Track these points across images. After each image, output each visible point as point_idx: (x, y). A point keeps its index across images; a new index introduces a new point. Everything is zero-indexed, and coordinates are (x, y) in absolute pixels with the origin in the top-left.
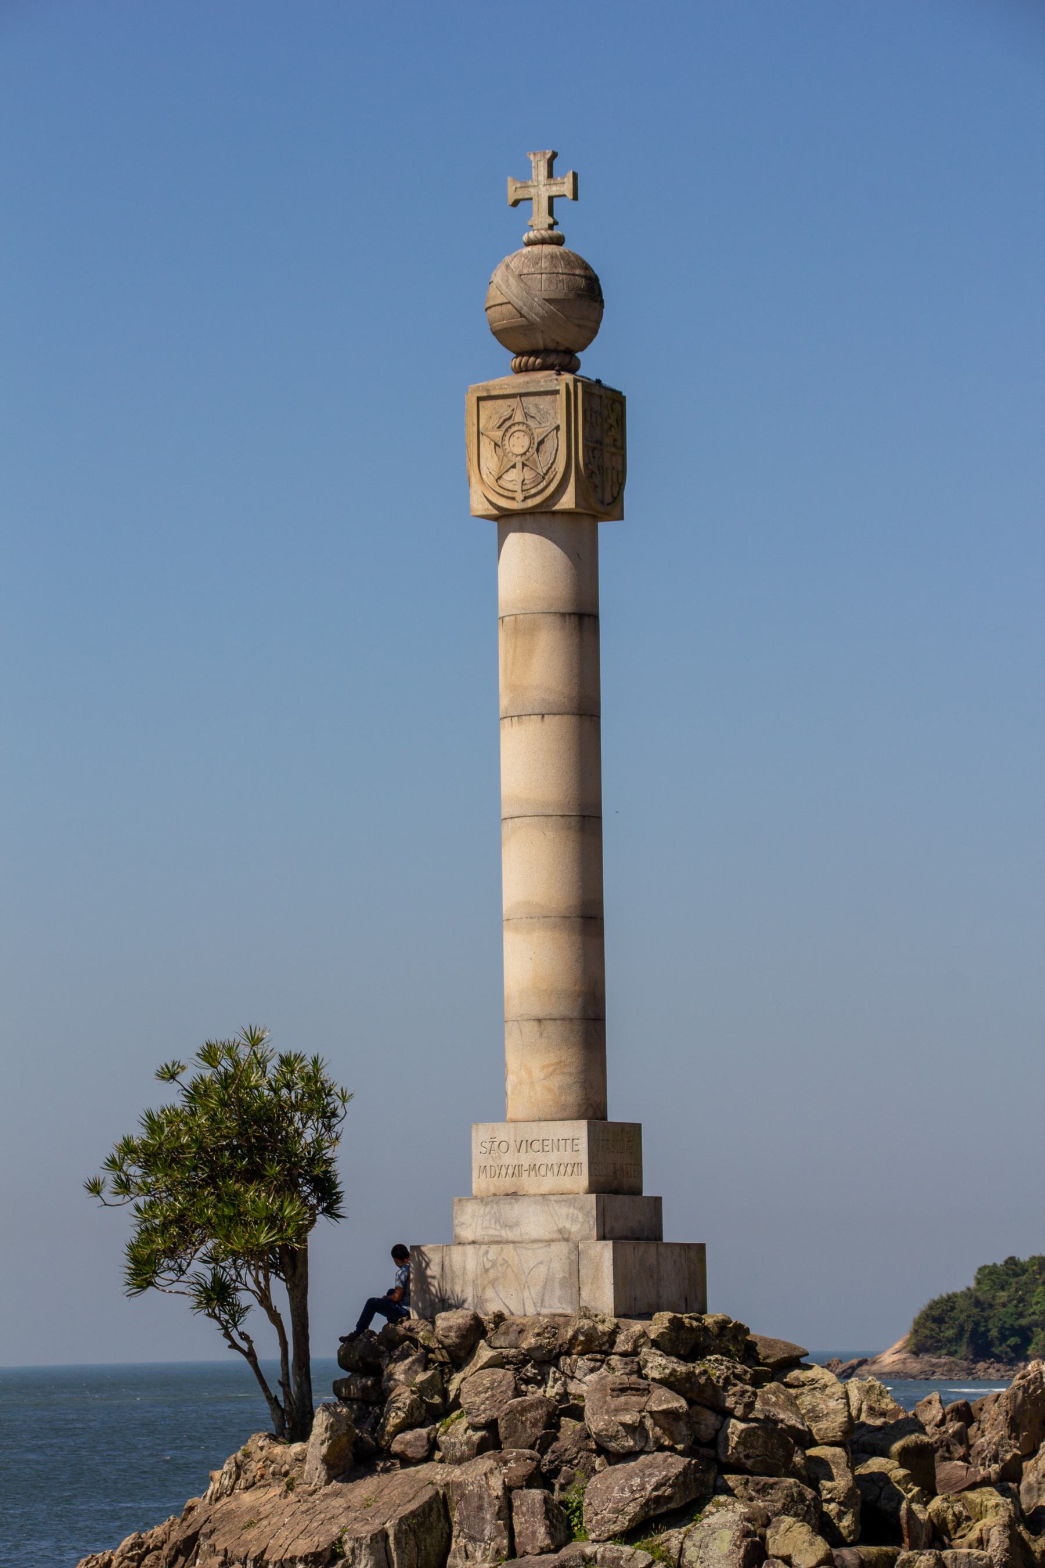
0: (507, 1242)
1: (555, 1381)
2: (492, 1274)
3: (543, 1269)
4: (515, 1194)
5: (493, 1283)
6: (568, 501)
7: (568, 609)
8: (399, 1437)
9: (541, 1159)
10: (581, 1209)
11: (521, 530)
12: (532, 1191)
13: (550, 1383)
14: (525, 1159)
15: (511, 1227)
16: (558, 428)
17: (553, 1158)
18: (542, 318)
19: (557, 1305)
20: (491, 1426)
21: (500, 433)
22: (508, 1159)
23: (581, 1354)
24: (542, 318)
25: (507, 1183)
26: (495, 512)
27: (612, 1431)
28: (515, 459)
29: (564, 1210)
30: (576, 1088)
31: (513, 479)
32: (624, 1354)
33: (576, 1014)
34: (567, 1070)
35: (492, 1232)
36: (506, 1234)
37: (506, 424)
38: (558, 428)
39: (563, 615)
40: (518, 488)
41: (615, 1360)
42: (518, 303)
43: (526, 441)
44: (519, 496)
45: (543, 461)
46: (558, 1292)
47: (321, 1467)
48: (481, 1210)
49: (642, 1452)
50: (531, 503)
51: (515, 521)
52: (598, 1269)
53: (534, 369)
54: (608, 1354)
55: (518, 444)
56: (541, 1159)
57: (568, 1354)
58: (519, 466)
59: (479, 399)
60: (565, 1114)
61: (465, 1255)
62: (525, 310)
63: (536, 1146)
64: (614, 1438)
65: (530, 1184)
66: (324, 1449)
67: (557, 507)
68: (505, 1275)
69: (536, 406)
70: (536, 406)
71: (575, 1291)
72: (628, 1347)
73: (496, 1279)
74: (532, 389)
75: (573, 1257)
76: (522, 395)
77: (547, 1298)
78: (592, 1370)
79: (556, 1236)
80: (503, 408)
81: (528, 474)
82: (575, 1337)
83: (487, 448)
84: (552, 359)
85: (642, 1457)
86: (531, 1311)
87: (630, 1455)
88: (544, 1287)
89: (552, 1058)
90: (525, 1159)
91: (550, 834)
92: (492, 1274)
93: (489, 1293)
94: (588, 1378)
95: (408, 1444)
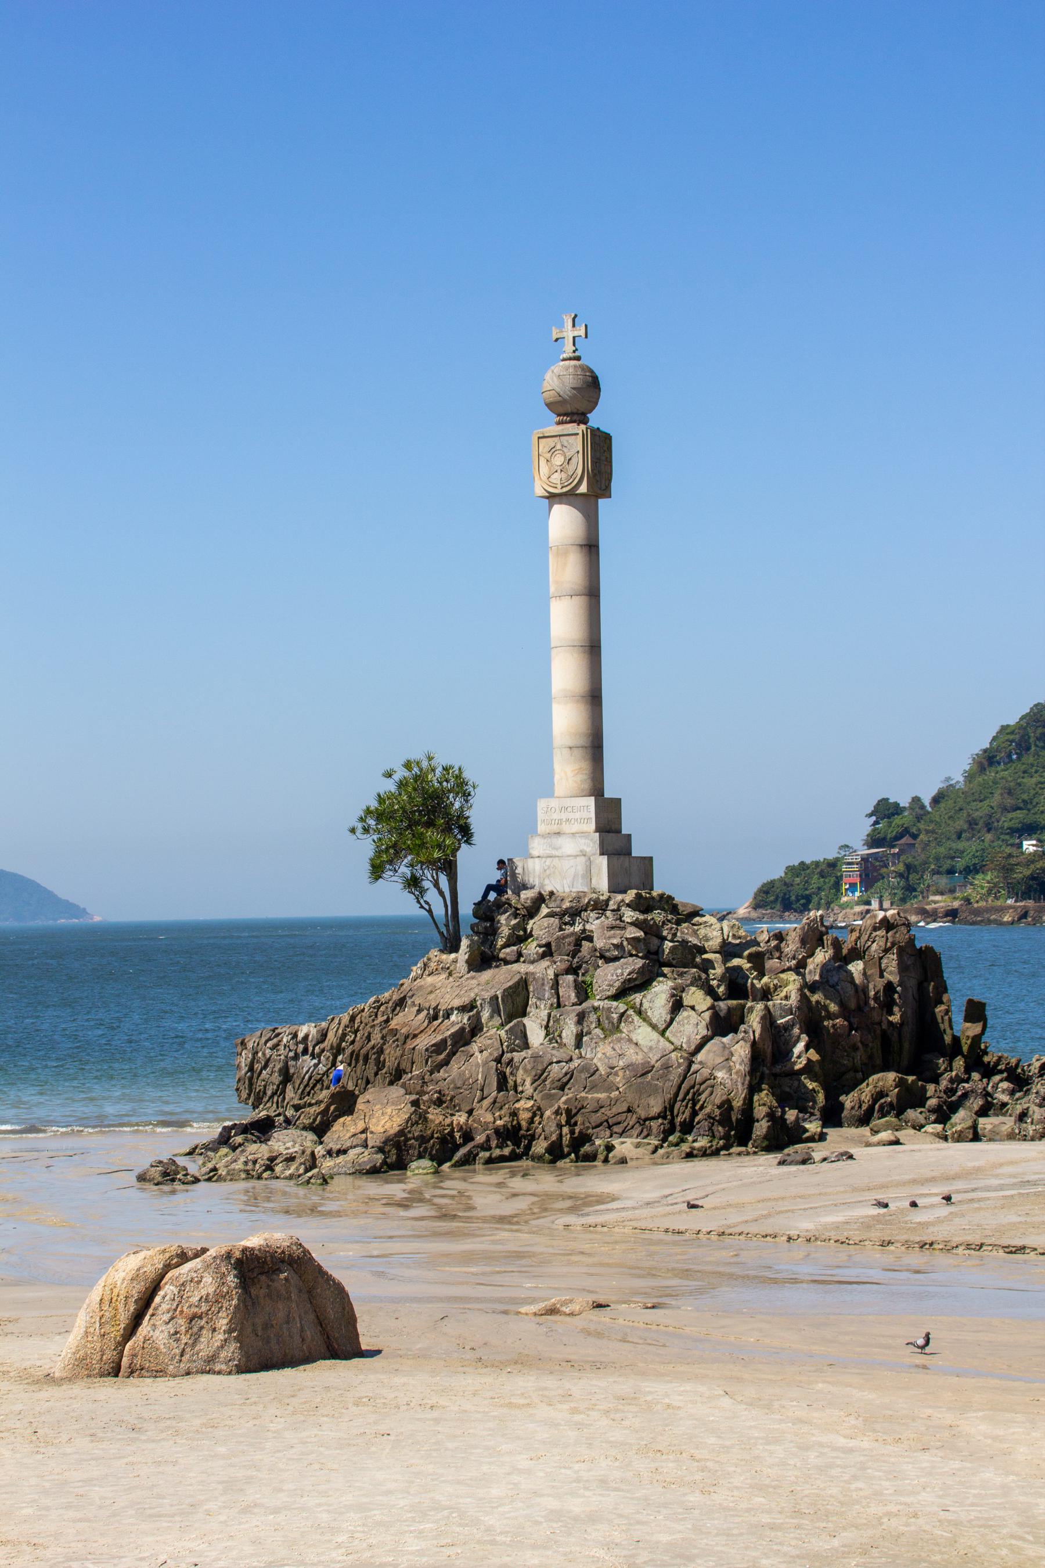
0: (555, 857)
1: (579, 923)
2: (548, 872)
3: (573, 870)
4: (559, 833)
5: (549, 876)
6: (583, 489)
7: (584, 543)
8: (503, 951)
9: (571, 816)
10: (592, 840)
11: (561, 503)
12: (567, 832)
13: (577, 924)
14: (564, 816)
15: (557, 849)
16: (578, 452)
17: (578, 815)
18: (570, 397)
19: (580, 887)
20: (548, 945)
21: (549, 455)
22: (555, 816)
23: (592, 910)
24: (570, 397)
25: (555, 828)
26: (547, 494)
27: (607, 947)
28: (556, 468)
29: (583, 841)
30: (589, 781)
31: (556, 478)
32: (613, 911)
33: (588, 744)
34: (584, 772)
35: (548, 852)
36: (555, 853)
37: (552, 450)
38: (578, 452)
39: (581, 546)
40: (559, 482)
41: (608, 913)
42: (558, 390)
43: (562, 459)
44: (559, 486)
45: (571, 469)
46: (580, 881)
47: (465, 965)
48: (542, 841)
49: (622, 957)
50: (565, 490)
51: (557, 499)
52: (600, 870)
53: (566, 423)
54: (605, 910)
55: (558, 460)
56: (571, 816)
57: (586, 910)
58: (559, 471)
59: (539, 438)
60: (584, 794)
61: (534, 863)
62: (561, 393)
63: (569, 809)
64: (608, 950)
65: (566, 828)
66: (467, 957)
67: (578, 492)
68: (554, 873)
69: (567, 441)
70: (567, 441)
71: (589, 880)
72: (615, 907)
73: (550, 875)
74: (565, 433)
75: (588, 864)
76: (560, 436)
77: (575, 883)
78: (597, 918)
79: (579, 853)
80: (551, 442)
81: (564, 475)
82: (589, 902)
83: (543, 462)
84: (575, 417)
85: (622, 960)
86: (567, 890)
87: (616, 959)
88: (573, 879)
89: (577, 766)
90: (564, 816)
91: (576, 655)
92: (548, 872)
93: (547, 882)
94: (596, 922)
95: (507, 954)
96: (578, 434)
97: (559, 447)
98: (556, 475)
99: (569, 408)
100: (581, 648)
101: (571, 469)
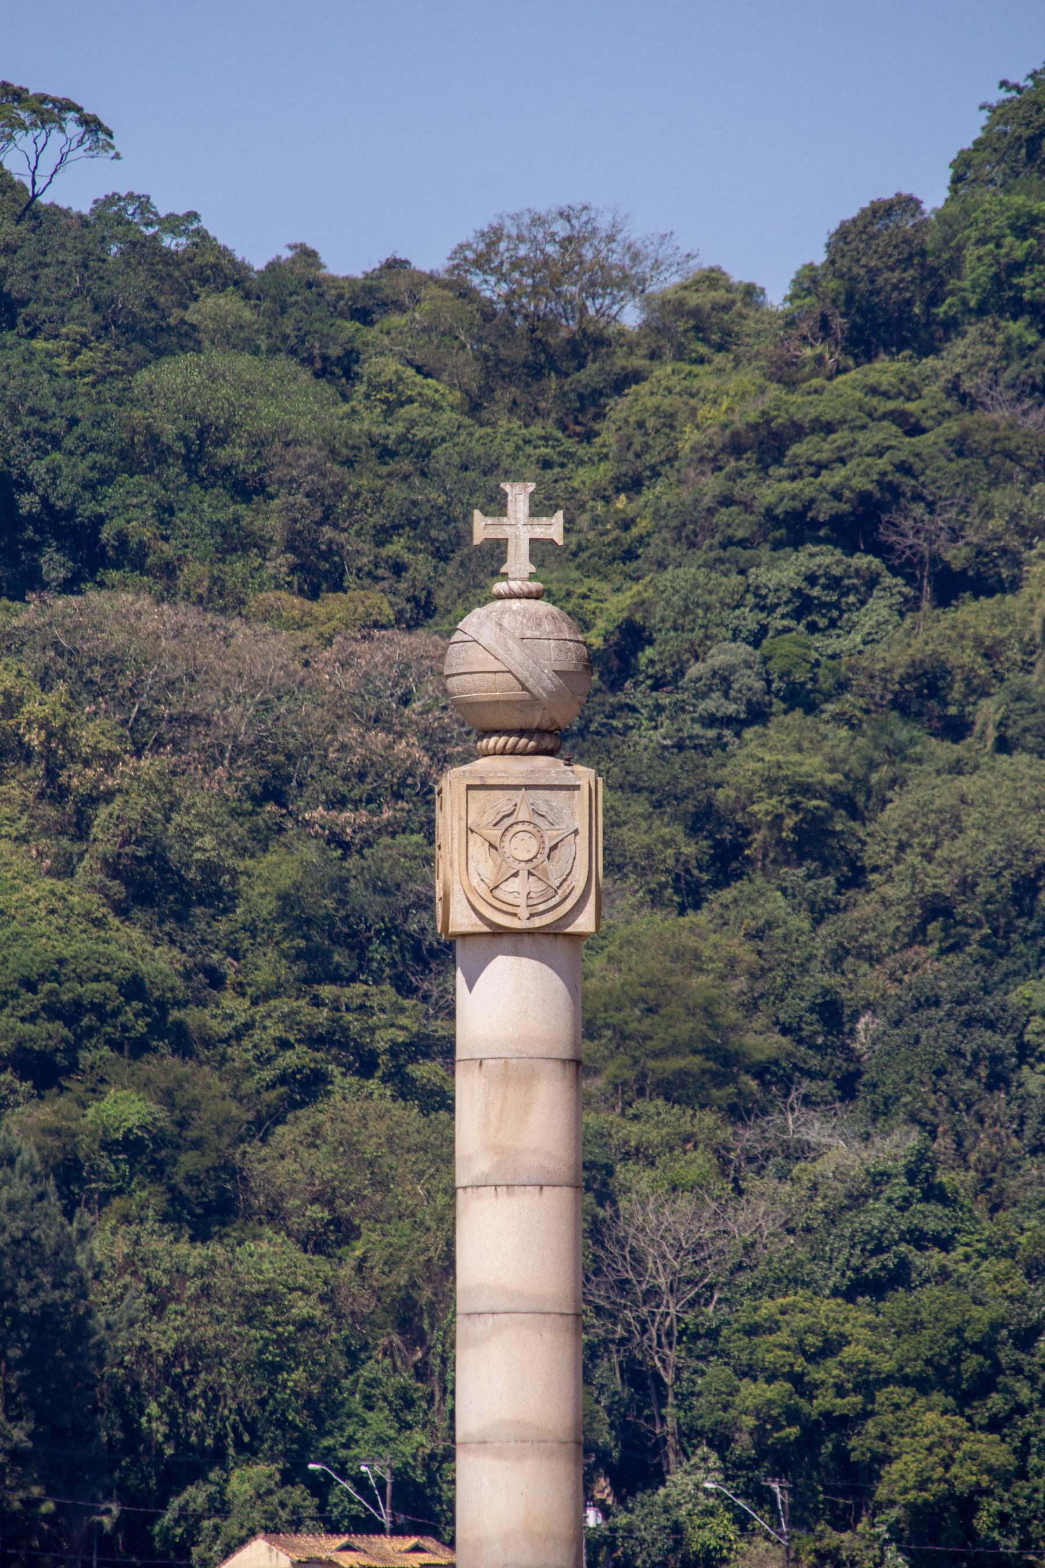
6: (585, 922)
11: (516, 953)
16: (576, 832)
18: (550, 693)
31: (515, 890)
37: (505, 820)
38: (576, 832)
40: (522, 901)
42: (522, 674)
43: (533, 846)
44: (523, 912)
45: (555, 871)
50: (538, 922)
51: (507, 942)
58: (523, 874)
59: (470, 787)
62: (530, 683)
67: (570, 929)
69: (547, 802)
70: (547, 802)
76: (528, 787)
80: (502, 801)
81: (535, 886)
91: (548, 1336)
96: (577, 787)
97: (523, 814)
98: (514, 885)
99: (536, 718)
100: (561, 1320)
101: (555, 871)
